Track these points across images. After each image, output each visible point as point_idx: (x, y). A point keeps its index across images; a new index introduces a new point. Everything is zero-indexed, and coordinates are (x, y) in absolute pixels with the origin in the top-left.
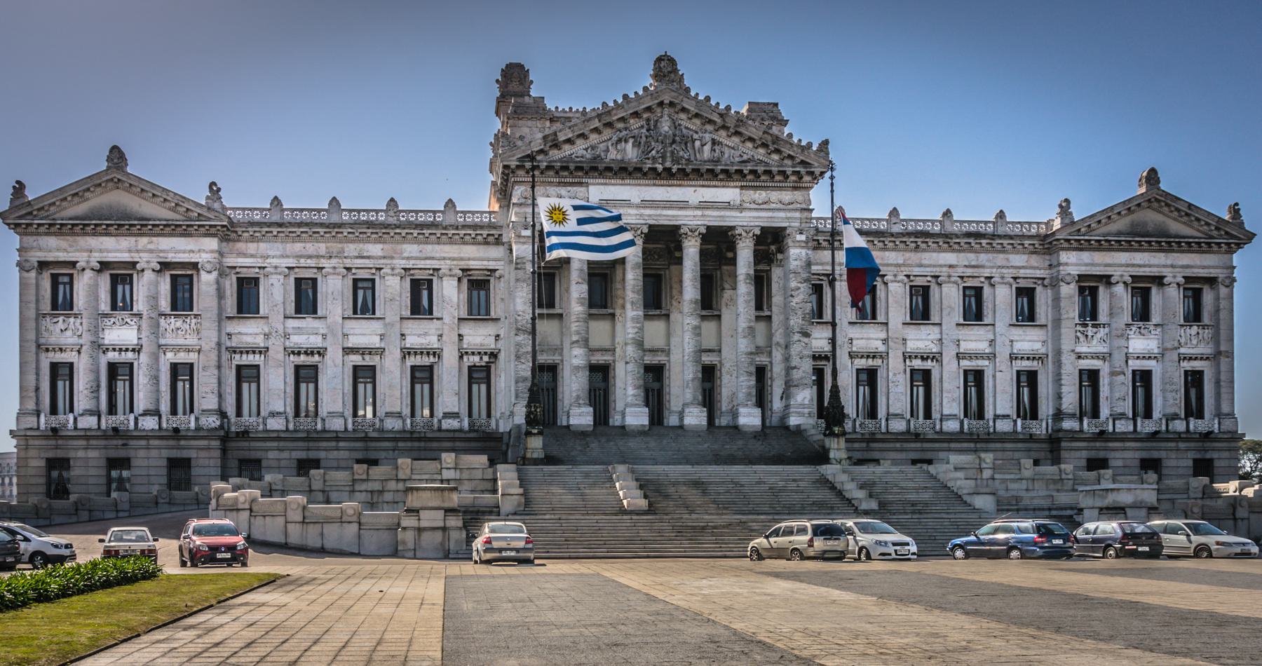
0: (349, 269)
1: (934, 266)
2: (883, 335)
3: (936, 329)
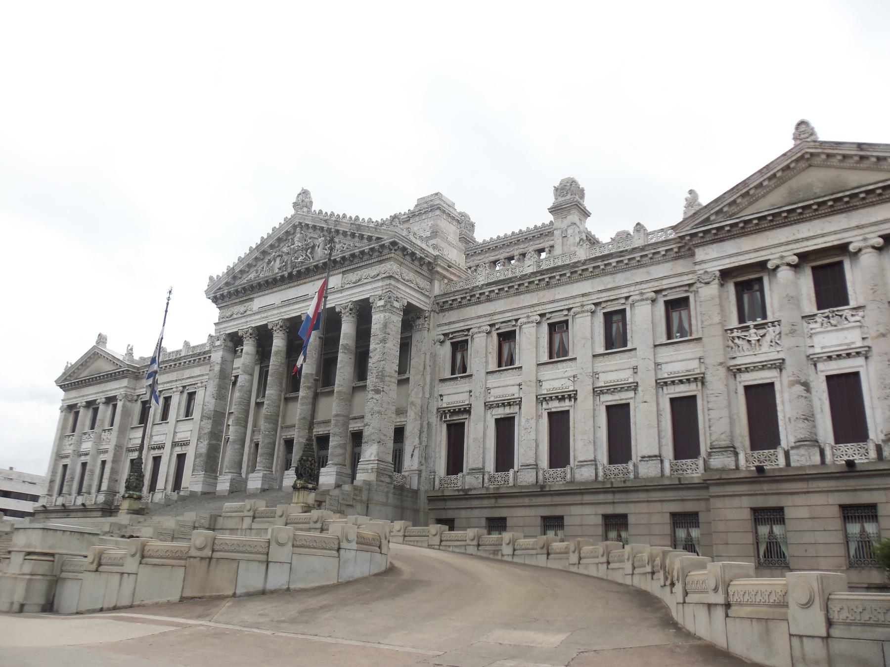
0: (184, 387)
1: (567, 299)
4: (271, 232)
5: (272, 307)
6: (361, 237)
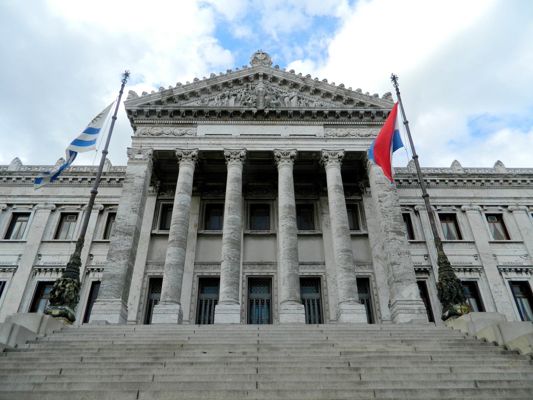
0: (10, 205)
1: (501, 198)
2: (474, 252)
3: (520, 246)
4: (225, 72)
5: (228, 136)
6: (350, 101)
